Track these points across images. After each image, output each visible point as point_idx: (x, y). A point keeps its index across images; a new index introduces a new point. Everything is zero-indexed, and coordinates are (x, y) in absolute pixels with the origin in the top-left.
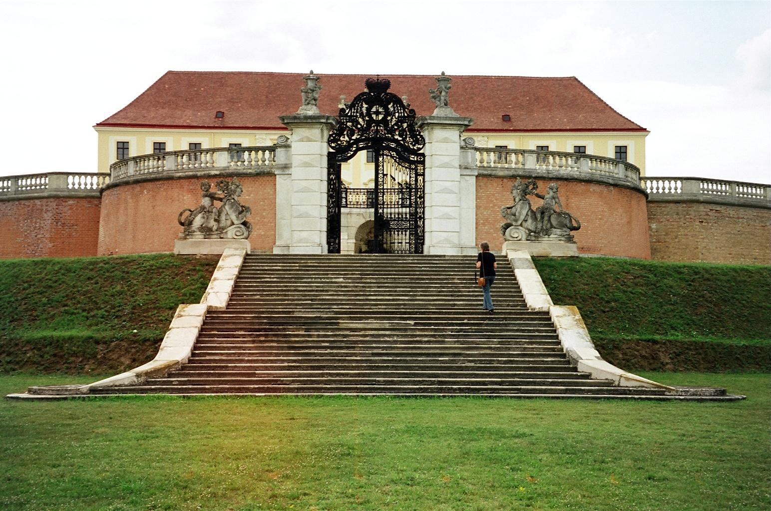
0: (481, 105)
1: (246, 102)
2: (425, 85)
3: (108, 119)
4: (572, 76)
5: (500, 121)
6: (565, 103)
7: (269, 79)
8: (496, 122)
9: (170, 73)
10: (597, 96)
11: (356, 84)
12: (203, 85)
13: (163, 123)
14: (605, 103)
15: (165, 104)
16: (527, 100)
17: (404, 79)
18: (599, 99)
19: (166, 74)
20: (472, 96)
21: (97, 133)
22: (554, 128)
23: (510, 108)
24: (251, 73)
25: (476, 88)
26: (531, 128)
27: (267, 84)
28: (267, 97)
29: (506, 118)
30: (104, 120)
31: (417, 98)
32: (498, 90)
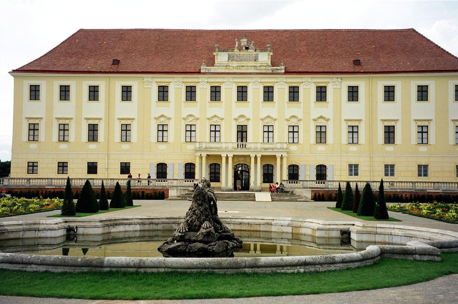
0: (334, 53)
1: (139, 51)
2: (287, 38)
3: (24, 66)
4: (410, 28)
5: (352, 65)
6: (406, 50)
7: (159, 35)
8: (348, 65)
9: (81, 30)
10: (434, 44)
11: (230, 37)
12: (106, 39)
13: (68, 69)
14: (442, 49)
15: (73, 54)
16: (374, 48)
17: (268, 33)
18: (437, 45)
19: (78, 31)
20: (326, 45)
21: (12, 78)
22: (399, 70)
23: (359, 54)
24: (146, 30)
25: (330, 39)
26: (380, 71)
27: (157, 38)
28: (156, 48)
29: (357, 63)
30: (20, 67)
31: (279, 47)
32: (348, 40)
